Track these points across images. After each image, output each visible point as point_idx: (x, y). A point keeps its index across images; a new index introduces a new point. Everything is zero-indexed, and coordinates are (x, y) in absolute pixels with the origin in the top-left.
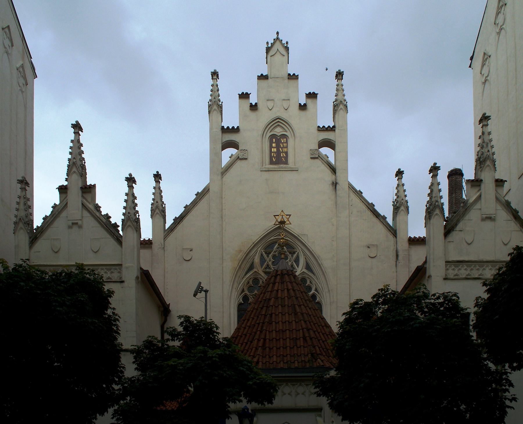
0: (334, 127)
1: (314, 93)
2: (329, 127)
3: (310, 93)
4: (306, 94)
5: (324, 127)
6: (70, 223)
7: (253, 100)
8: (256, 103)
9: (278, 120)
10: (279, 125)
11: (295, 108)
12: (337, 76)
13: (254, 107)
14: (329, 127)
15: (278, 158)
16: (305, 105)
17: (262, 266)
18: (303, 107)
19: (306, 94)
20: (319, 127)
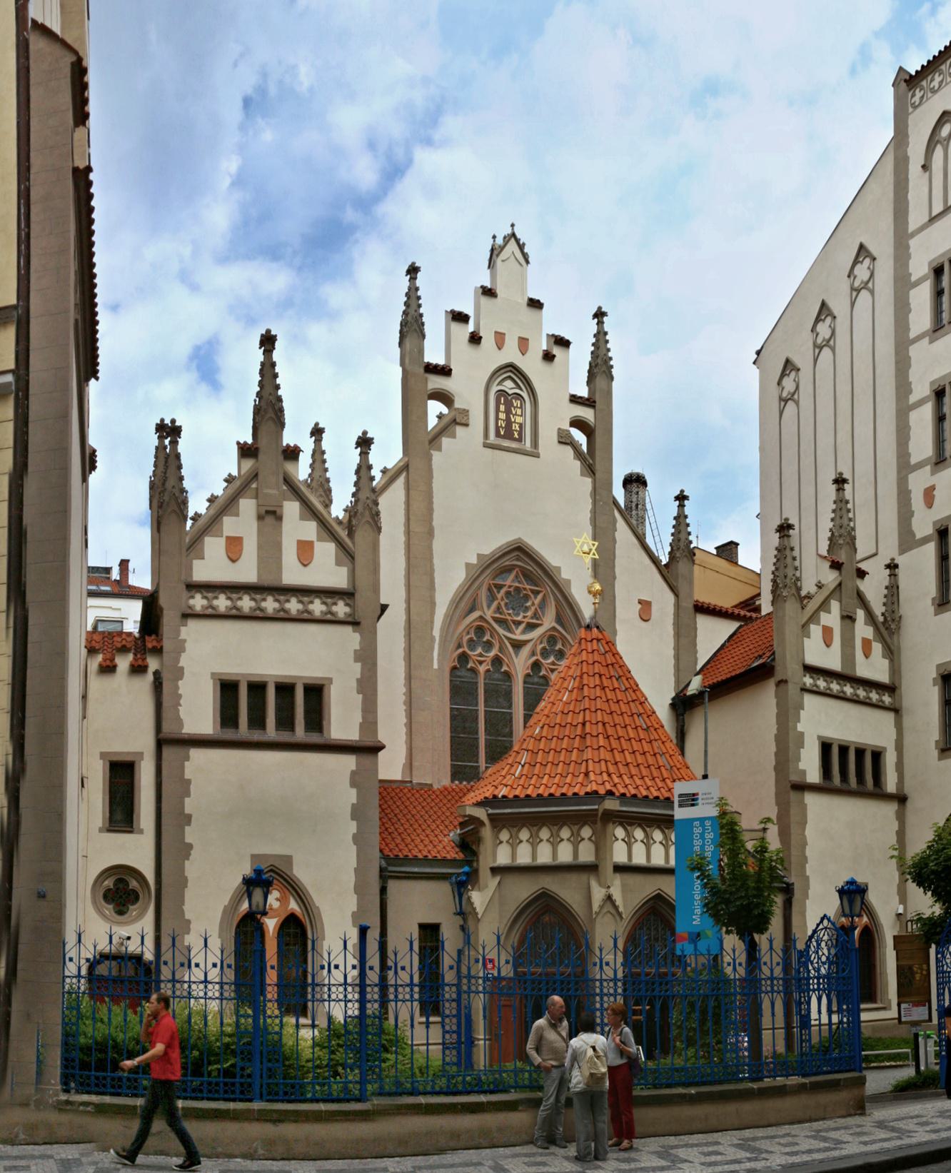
6: (263, 510)
15: (509, 436)
17: (489, 607)
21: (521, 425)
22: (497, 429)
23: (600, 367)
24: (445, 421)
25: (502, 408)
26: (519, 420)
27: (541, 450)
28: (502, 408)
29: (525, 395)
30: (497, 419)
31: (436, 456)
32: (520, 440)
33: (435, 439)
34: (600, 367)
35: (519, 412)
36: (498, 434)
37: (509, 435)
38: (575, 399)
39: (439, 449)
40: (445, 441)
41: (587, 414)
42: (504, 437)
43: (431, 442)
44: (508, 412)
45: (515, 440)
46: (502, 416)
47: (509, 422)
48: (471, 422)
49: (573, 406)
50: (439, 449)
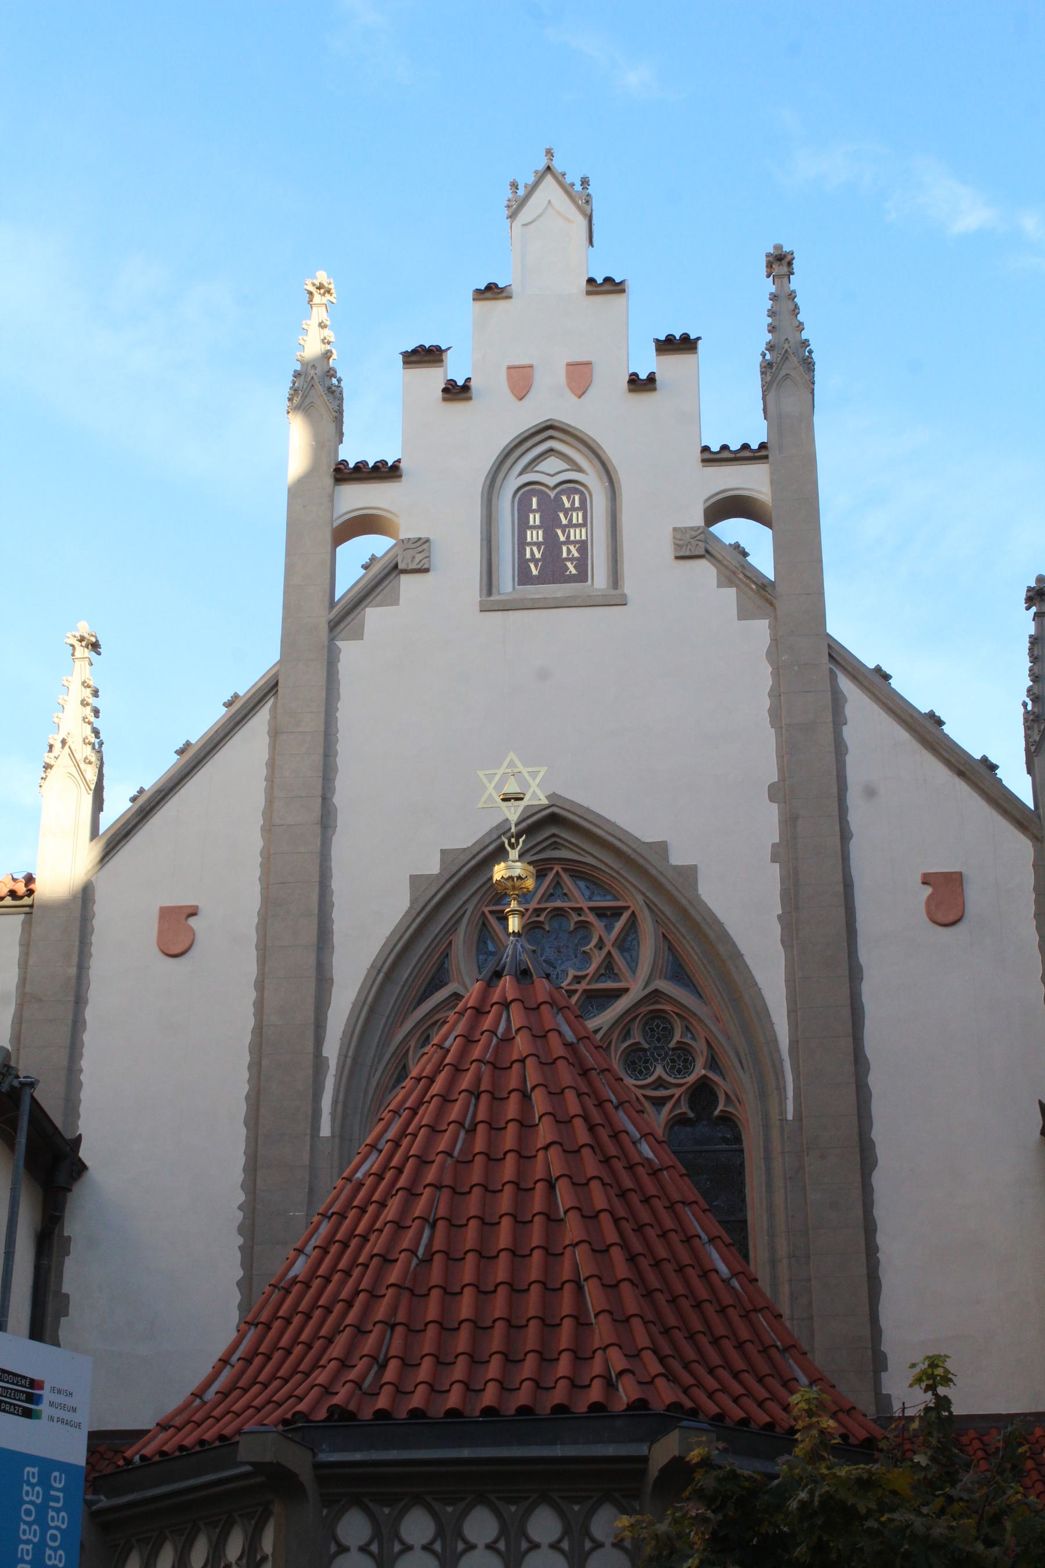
0: (763, 446)
1: (685, 338)
2: (745, 447)
3: (670, 340)
4: (657, 341)
5: (725, 448)
7: (456, 369)
8: (468, 379)
9: (550, 432)
10: (551, 451)
11: (610, 383)
12: (770, 265)
13: (456, 392)
14: (745, 447)
16: (651, 379)
18: (641, 384)
19: (657, 341)
20: (706, 449)
21: (583, 546)
22: (522, 567)
23: (788, 367)
24: (375, 569)
25: (535, 519)
26: (576, 534)
27: (629, 586)
28: (535, 519)
29: (592, 479)
30: (522, 543)
31: (349, 650)
32: (582, 576)
33: (345, 616)
34: (788, 367)
35: (577, 517)
36: (524, 577)
37: (553, 570)
38: (711, 457)
39: (358, 635)
40: (373, 616)
41: (753, 481)
42: (540, 580)
43: (334, 626)
44: (550, 524)
45: (572, 579)
46: (535, 536)
47: (551, 545)
48: (438, 557)
49: (713, 471)
50: (358, 635)
